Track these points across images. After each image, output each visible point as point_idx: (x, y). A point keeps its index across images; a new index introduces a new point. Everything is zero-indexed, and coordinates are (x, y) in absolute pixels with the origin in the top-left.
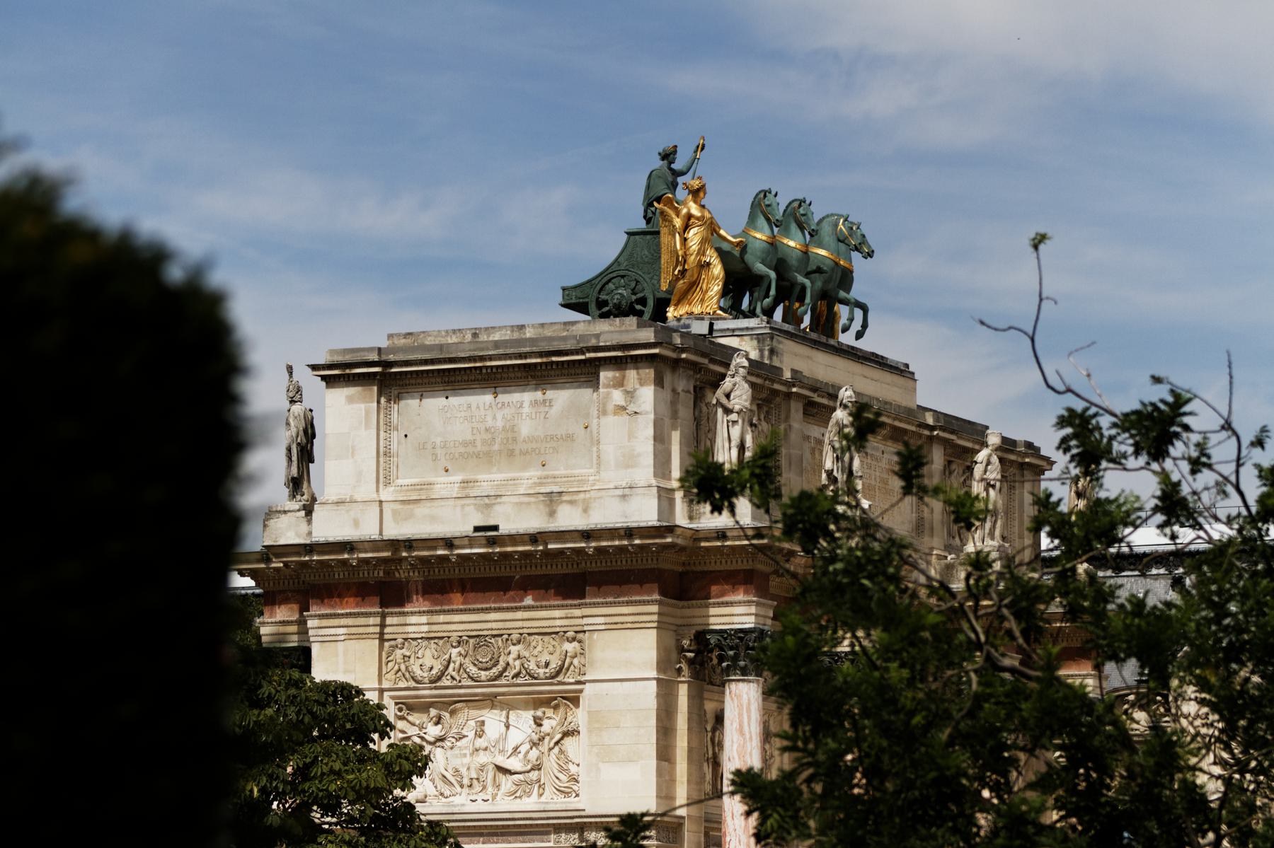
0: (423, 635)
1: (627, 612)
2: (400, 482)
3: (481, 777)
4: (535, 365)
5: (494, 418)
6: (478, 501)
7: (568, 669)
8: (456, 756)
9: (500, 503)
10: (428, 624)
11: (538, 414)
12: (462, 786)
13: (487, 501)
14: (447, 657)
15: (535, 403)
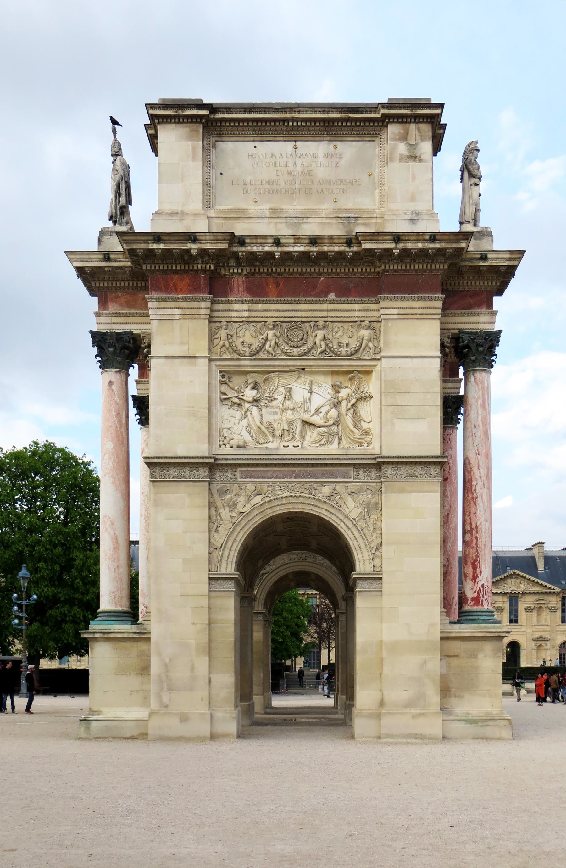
0: (244, 319)
1: (417, 306)
2: (218, 207)
3: (291, 430)
4: (337, 120)
5: (295, 164)
6: (288, 220)
7: (364, 349)
8: (270, 414)
9: (307, 223)
10: (249, 311)
11: (330, 163)
12: (274, 436)
13: (295, 220)
14: (265, 335)
15: (327, 155)
